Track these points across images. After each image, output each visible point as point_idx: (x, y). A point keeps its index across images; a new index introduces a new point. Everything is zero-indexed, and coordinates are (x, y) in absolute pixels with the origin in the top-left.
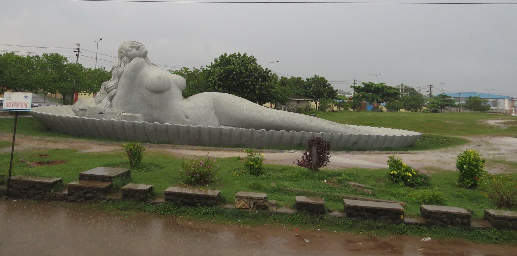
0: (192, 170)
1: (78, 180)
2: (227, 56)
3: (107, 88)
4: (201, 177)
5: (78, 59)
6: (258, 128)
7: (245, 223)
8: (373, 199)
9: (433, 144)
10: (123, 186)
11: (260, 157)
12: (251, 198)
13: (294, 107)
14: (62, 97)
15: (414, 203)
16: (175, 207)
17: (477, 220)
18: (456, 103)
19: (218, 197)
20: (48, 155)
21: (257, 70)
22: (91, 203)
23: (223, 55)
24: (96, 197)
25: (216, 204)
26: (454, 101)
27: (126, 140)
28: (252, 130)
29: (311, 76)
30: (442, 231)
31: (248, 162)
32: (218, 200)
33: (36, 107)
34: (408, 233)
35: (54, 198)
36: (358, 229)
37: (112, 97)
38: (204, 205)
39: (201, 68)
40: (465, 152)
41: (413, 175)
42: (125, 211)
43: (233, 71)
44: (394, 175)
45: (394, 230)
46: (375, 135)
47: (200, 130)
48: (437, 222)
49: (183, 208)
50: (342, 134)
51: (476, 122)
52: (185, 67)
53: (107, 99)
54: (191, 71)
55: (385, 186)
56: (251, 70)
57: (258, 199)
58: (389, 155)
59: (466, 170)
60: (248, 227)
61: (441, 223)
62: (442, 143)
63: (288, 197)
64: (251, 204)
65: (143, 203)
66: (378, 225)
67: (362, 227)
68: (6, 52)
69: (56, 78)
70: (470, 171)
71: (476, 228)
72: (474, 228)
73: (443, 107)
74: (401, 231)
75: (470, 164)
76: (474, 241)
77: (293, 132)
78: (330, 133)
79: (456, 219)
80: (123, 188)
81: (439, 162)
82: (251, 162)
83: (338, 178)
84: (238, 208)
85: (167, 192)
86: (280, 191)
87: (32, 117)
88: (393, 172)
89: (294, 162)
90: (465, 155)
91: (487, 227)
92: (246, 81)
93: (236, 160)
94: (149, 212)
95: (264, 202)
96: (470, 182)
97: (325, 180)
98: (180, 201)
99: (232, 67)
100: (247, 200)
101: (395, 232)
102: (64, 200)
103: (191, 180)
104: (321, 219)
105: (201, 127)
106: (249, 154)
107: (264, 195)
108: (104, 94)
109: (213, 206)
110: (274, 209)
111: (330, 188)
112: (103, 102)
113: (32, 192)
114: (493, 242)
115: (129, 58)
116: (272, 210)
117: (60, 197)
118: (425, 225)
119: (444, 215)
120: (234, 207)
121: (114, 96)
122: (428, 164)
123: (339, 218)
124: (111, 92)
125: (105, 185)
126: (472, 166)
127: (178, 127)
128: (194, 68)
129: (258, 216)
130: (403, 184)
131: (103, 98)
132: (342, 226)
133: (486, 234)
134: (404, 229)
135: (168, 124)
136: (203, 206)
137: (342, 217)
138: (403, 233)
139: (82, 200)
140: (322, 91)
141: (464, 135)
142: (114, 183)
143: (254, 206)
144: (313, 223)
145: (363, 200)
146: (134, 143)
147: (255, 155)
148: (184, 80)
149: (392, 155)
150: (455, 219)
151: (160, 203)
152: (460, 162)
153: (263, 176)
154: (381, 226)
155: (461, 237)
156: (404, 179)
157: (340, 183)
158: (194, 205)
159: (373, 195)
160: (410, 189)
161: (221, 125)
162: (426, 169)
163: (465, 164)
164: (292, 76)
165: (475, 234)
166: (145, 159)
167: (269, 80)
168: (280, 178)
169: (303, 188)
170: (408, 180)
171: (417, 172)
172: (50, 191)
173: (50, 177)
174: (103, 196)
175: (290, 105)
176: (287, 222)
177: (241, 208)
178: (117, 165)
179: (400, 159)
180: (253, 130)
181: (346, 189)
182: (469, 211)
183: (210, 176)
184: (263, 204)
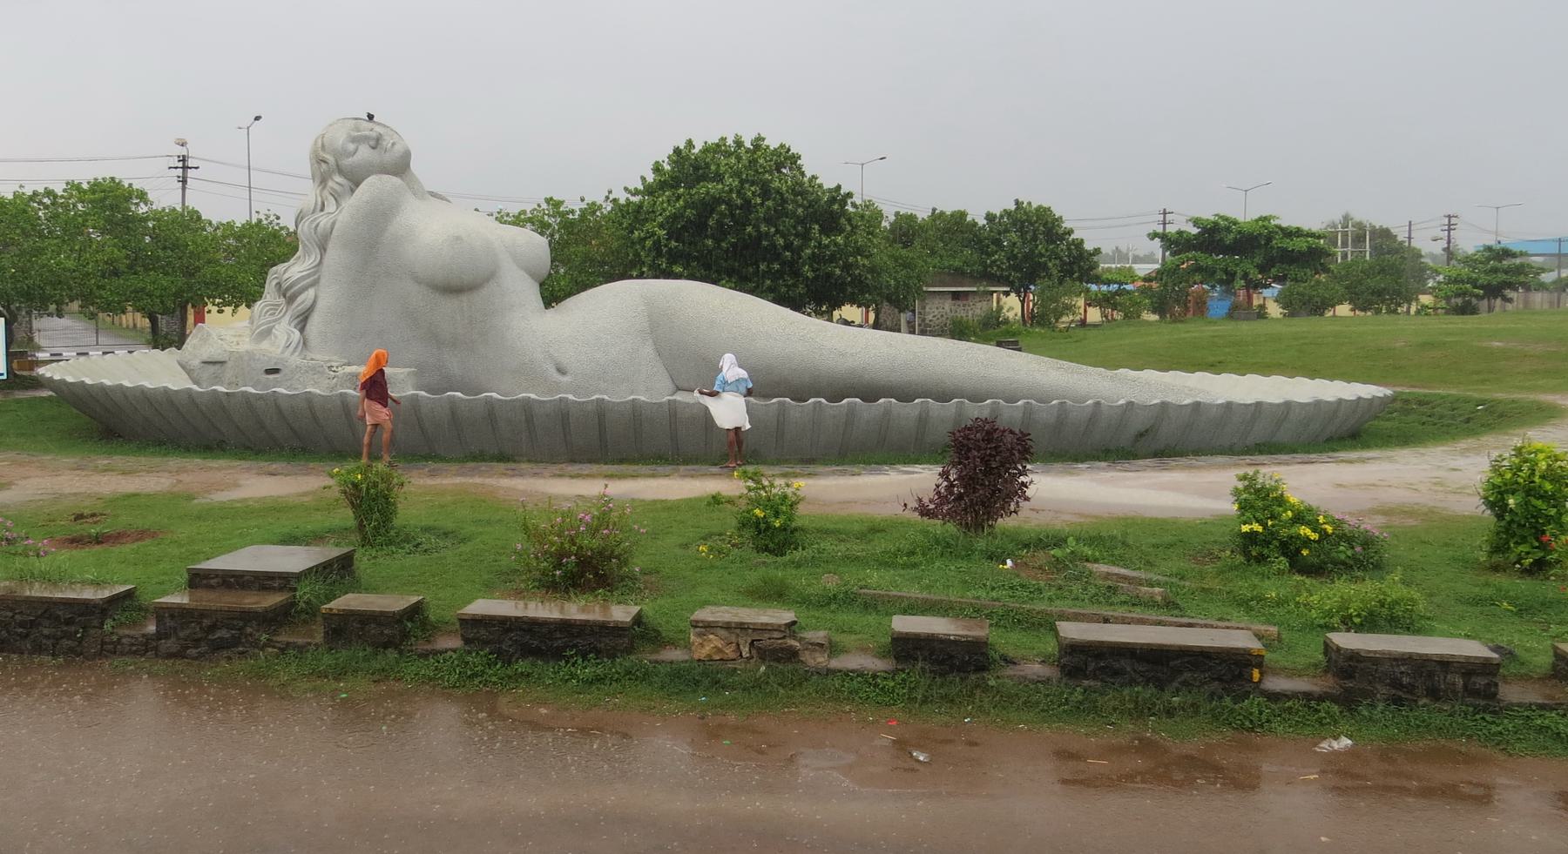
0: (552, 544)
3: (285, 286)
4: (585, 563)
6: (800, 397)
7: (721, 707)
8: (1163, 618)
11: (789, 491)
12: (742, 627)
16: (497, 664)
17: (1525, 678)
25: (630, 650)
28: (779, 402)
30: (1393, 717)
31: (748, 512)
32: (640, 633)
34: (1273, 725)
41: (1324, 535)
42: (337, 679)
45: (1224, 717)
47: (601, 412)
48: (1377, 689)
49: (522, 666)
50: (1098, 404)
60: (732, 718)
61: (1394, 691)
63: (872, 619)
64: (741, 647)
67: (1115, 709)
71: (1520, 705)
72: (1510, 706)
74: (1251, 721)
78: (1054, 402)
79: (1449, 677)
82: (757, 511)
84: (699, 660)
89: (905, 505)
93: (709, 504)
95: (784, 637)
97: (1009, 562)
98: (510, 643)
100: (730, 633)
101: (1230, 724)
103: (554, 575)
104: (977, 686)
105: (603, 399)
106: (751, 484)
107: (784, 616)
108: (279, 305)
110: (820, 659)
116: (811, 662)
120: (687, 657)
121: (312, 311)
129: (767, 683)
130: (1282, 567)
132: (1046, 708)
134: (1261, 713)
135: (494, 395)
136: (584, 658)
143: (754, 652)
147: (772, 485)
148: (544, 241)
150: (1445, 677)
153: (797, 555)
155: (1462, 735)
158: (557, 654)
159: (1169, 604)
161: (679, 389)
169: (929, 587)
171: (1338, 523)
176: (861, 698)
177: (712, 660)
181: (1076, 588)
183: (614, 560)
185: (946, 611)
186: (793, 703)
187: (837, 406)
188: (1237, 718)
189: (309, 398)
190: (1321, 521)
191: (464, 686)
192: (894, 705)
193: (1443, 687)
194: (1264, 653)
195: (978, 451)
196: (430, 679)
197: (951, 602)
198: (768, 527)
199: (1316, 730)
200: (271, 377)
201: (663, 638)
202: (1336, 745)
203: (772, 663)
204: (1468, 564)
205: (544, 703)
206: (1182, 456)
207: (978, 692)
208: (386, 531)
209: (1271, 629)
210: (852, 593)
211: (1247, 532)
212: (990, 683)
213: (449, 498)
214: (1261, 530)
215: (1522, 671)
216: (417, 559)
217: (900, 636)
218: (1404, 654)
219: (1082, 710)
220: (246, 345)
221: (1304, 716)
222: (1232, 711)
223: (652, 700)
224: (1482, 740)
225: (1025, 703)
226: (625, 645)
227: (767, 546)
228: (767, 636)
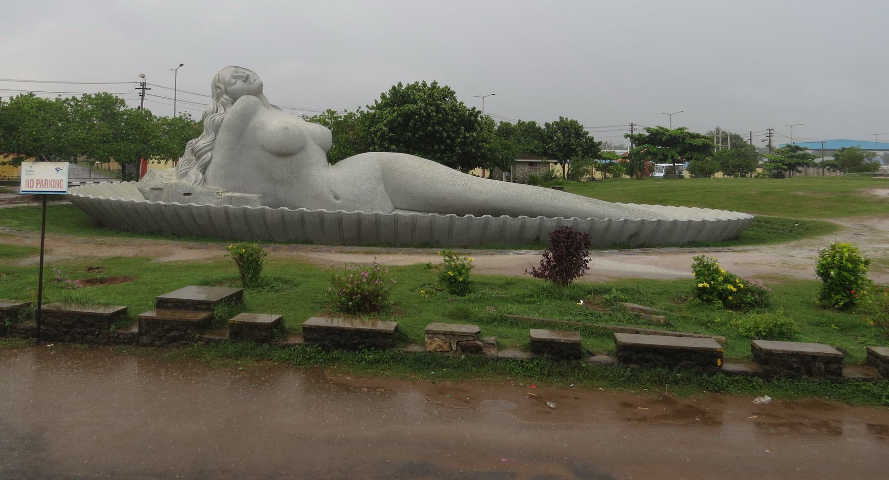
0: (347, 288)
2: (403, 88)
3: (196, 150)
5: (144, 100)
6: (461, 214)
7: (443, 377)
8: (668, 332)
9: (775, 233)
10: (232, 318)
11: (466, 263)
12: (452, 334)
13: (524, 174)
14: (120, 167)
15: (740, 337)
16: (322, 352)
17: (855, 365)
18: (817, 161)
19: (396, 333)
20: (102, 268)
21: (456, 111)
22: (178, 347)
23: (396, 86)
24: (186, 337)
25: (393, 346)
26: (813, 156)
27: (233, 238)
28: (450, 216)
29: (553, 118)
30: (790, 385)
31: (445, 273)
32: (397, 337)
33: (75, 187)
34: (730, 389)
35: (116, 340)
36: (642, 384)
38: (372, 346)
39: (358, 110)
40: (833, 247)
41: (739, 288)
42: (236, 359)
43: (416, 114)
44: (703, 289)
45: (704, 384)
46: (671, 220)
47: (359, 220)
48: (781, 370)
49: (335, 353)
50: (610, 220)
51: (855, 192)
52: (330, 110)
53: (197, 170)
54: (340, 117)
55: (689, 308)
56: (446, 111)
57: (464, 335)
58: (696, 255)
59: (834, 279)
60: (449, 383)
61: (789, 372)
62: (791, 231)
63: (516, 330)
64: (452, 345)
65: (266, 346)
66: (676, 377)
67: (648, 380)
68: (21, 92)
69: (108, 135)
70: (841, 280)
71: (853, 379)
72: (848, 380)
73: (792, 167)
74: (718, 387)
75: (842, 268)
76: (848, 402)
78: (589, 219)
80: (231, 321)
81: (786, 266)
82: (450, 273)
83: (604, 296)
84: (430, 352)
85: (307, 327)
86: (502, 320)
87: (71, 203)
89: (526, 271)
90: (833, 252)
91: (871, 377)
92: (438, 131)
93: (425, 268)
94: (277, 360)
95: (474, 340)
96: (841, 299)
97: (581, 301)
99: (412, 107)
102: (133, 342)
103: (348, 305)
104: (576, 367)
105: (361, 213)
106: (447, 258)
107: (474, 328)
109: (387, 348)
110: (493, 352)
111: (591, 314)
113: (78, 330)
114: (883, 403)
115: (231, 97)
116: (488, 353)
117: (125, 339)
118: (760, 376)
119: (793, 357)
120: (423, 350)
121: (209, 163)
122: (766, 269)
123: (608, 365)
124: (203, 157)
125: (202, 315)
126: (845, 272)
127: (321, 214)
128: (346, 111)
129: (466, 364)
130: (720, 306)
131: (189, 168)
132: (612, 379)
133: (871, 390)
134: (723, 382)
135: (305, 209)
136: (369, 349)
137: (612, 363)
138: (720, 389)
140: (573, 144)
141: (831, 217)
143: (458, 347)
144: (562, 375)
145: (649, 334)
146: (247, 243)
147: (458, 259)
148: (329, 132)
149: (700, 255)
150: (815, 364)
151: (295, 345)
152: (823, 265)
153: (472, 296)
154: (682, 378)
155: (826, 395)
156: (723, 295)
157: (608, 306)
158: (353, 348)
159: (667, 324)
160: (734, 313)
161: (396, 208)
162: (762, 278)
163: (832, 268)
164: (520, 121)
165: (850, 390)
166: (267, 271)
167: (479, 129)
169: (543, 314)
170: (730, 298)
172: (109, 328)
173: (107, 305)
174: (198, 336)
175: (516, 171)
176: (515, 373)
177: (435, 352)
178: (220, 282)
179: (714, 261)
180: (453, 216)
181: (619, 315)
182: (838, 349)
183: (380, 297)
184: (473, 343)
185: (554, 327)
186: (480, 375)
187: (479, 219)
188: (711, 385)
189: (208, 209)
191: (305, 364)
194: (723, 351)
196: (287, 360)
197: (556, 322)
198: (456, 281)
200: (187, 197)
202: (763, 400)
203: (468, 354)
205: (349, 374)
207: (576, 371)
210: (504, 316)
212: (582, 365)
214: (708, 286)
216: (274, 295)
219: (633, 380)
220: (174, 181)
222: (708, 382)
224: (836, 397)
225: (601, 376)
226: (390, 343)
228: (465, 339)
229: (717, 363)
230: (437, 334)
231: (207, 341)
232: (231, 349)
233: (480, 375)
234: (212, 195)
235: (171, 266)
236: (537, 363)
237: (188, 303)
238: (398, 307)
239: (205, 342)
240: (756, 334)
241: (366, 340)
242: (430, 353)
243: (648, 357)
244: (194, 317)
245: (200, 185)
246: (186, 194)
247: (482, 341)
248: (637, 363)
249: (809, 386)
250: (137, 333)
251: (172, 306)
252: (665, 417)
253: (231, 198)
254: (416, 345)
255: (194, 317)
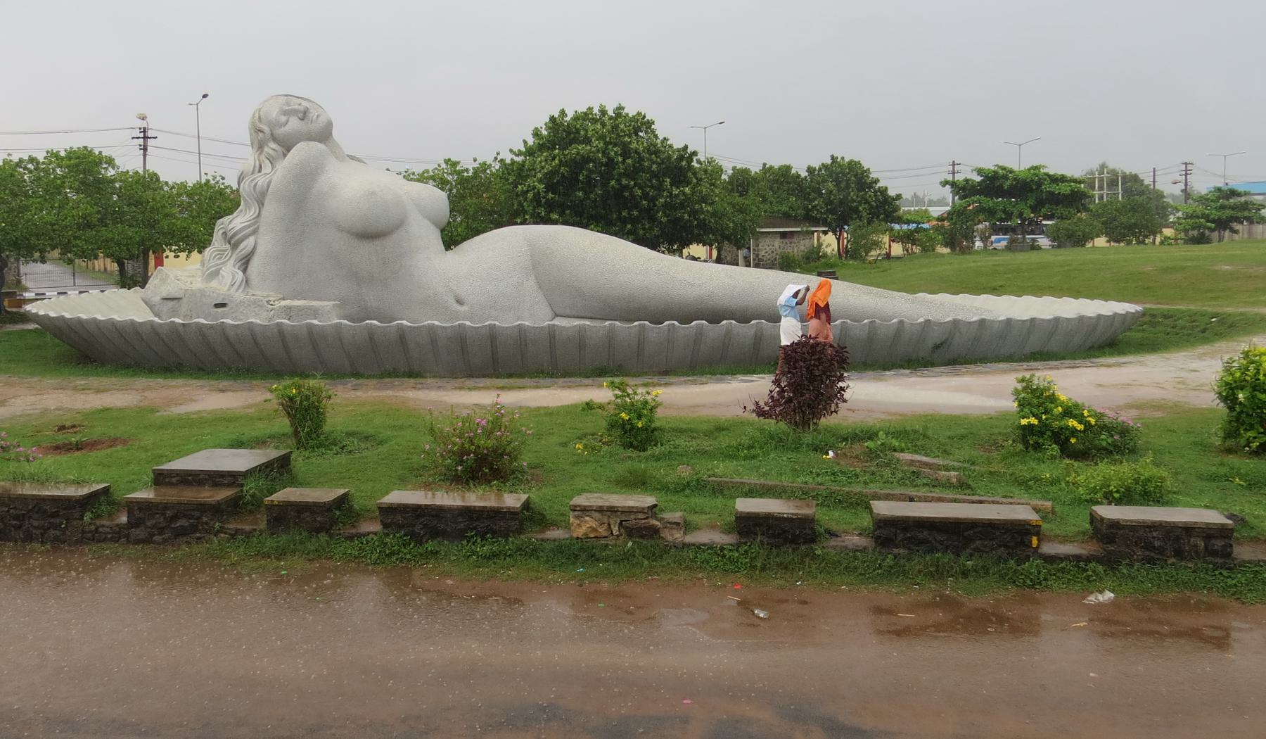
0: (454, 444)
1: (151, 486)
3: (230, 234)
7: (596, 576)
8: (958, 496)
11: (649, 398)
12: (612, 510)
16: (410, 544)
19: (525, 512)
20: (80, 426)
22: (188, 543)
25: (520, 530)
27: (279, 375)
28: (640, 325)
30: (1148, 574)
31: (616, 415)
32: (529, 517)
34: (1049, 583)
37: (245, 257)
41: (1088, 427)
42: (278, 559)
45: (1009, 576)
46: (1001, 319)
47: (493, 336)
48: (1134, 551)
49: (430, 545)
50: (901, 322)
53: (234, 266)
57: (630, 511)
60: (605, 585)
61: (1147, 553)
63: (719, 501)
64: (612, 526)
65: (323, 537)
67: (920, 572)
71: (1250, 562)
72: (1243, 564)
74: (1031, 580)
75: (1257, 388)
77: (757, 323)
78: (866, 321)
80: (268, 501)
82: (623, 415)
84: (578, 538)
85: (384, 506)
88: (1028, 421)
89: (745, 408)
93: (583, 409)
95: (647, 518)
97: (831, 453)
98: (421, 526)
101: (1015, 582)
102: (120, 538)
103: (456, 470)
104: (807, 555)
105: (495, 325)
106: (618, 392)
107: (648, 500)
108: (225, 251)
109: (511, 535)
110: (678, 536)
112: (224, 273)
115: (283, 147)
116: (670, 538)
118: (1099, 560)
120: (567, 536)
123: (857, 550)
124: (242, 246)
125: (223, 494)
127: (432, 329)
129: (634, 556)
130: (1055, 453)
132: (863, 572)
134: (1039, 572)
135: (405, 322)
136: (483, 538)
137: (865, 548)
139: (166, 536)
142: (245, 488)
143: (622, 530)
145: (930, 502)
146: (300, 379)
147: (635, 393)
148: (444, 195)
150: (1189, 541)
151: (368, 534)
153: (657, 450)
158: (460, 535)
159: (963, 485)
161: (557, 315)
165: (1243, 579)
168: (703, 453)
169: (765, 475)
171: (1099, 416)
174: (217, 525)
176: (711, 567)
177: (588, 538)
178: (259, 443)
180: (645, 324)
181: (887, 473)
183: (506, 457)
184: (644, 524)
185: (780, 494)
186: (656, 572)
188: (1020, 577)
189: (251, 326)
190: (1085, 415)
192: (738, 572)
193: (1187, 548)
194: (1041, 523)
195: (804, 362)
196: (356, 558)
197: (783, 486)
198: (633, 428)
199: (1085, 586)
200: (220, 310)
201: (547, 520)
202: (1101, 598)
204: (1204, 447)
205: (450, 575)
206: (971, 364)
207: (807, 560)
208: (317, 435)
209: (1046, 504)
210: (702, 480)
211: (1025, 425)
212: (817, 552)
213: (369, 408)
215: (1252, 534)
216: (343, 459)
217: (743, 515)
218: (1155, 522)
219: (894, 573)
220: (198, 284)
221: (1075, 575)
222: (1015, 572)
223: (539, 572)
224: (1221, 591)
225: (846, 568)
226: (516, 526)
227: (631, 443)
228: (633, 517)
229: (1031, 544)
230: (588, 510)
231: (233, 532)
232: (270, 543)
233: (656, 572)
234: (259, 305)
235: (189, 419)
236: (746, 551)
237: (201, 477)
238: (538, 471)
239: (230, 534)
240: (1104, 497)
241: (477, 523)
242: (579, 541)
243: (921, 536)
244: (211, 497)
245: (240, 291)
246: (217, 306)
247: (661, 520)
248: (905, 547)
249: (1177, 574)
250: (124, 525)
251: (178, 481)
252: (939, 627)
253: (290, 308)
254: (558, 529)
255: (211, 497)
